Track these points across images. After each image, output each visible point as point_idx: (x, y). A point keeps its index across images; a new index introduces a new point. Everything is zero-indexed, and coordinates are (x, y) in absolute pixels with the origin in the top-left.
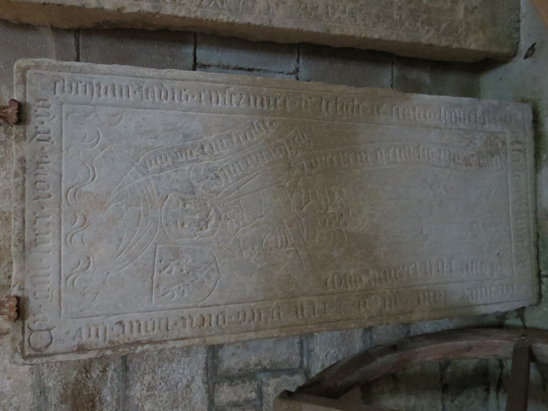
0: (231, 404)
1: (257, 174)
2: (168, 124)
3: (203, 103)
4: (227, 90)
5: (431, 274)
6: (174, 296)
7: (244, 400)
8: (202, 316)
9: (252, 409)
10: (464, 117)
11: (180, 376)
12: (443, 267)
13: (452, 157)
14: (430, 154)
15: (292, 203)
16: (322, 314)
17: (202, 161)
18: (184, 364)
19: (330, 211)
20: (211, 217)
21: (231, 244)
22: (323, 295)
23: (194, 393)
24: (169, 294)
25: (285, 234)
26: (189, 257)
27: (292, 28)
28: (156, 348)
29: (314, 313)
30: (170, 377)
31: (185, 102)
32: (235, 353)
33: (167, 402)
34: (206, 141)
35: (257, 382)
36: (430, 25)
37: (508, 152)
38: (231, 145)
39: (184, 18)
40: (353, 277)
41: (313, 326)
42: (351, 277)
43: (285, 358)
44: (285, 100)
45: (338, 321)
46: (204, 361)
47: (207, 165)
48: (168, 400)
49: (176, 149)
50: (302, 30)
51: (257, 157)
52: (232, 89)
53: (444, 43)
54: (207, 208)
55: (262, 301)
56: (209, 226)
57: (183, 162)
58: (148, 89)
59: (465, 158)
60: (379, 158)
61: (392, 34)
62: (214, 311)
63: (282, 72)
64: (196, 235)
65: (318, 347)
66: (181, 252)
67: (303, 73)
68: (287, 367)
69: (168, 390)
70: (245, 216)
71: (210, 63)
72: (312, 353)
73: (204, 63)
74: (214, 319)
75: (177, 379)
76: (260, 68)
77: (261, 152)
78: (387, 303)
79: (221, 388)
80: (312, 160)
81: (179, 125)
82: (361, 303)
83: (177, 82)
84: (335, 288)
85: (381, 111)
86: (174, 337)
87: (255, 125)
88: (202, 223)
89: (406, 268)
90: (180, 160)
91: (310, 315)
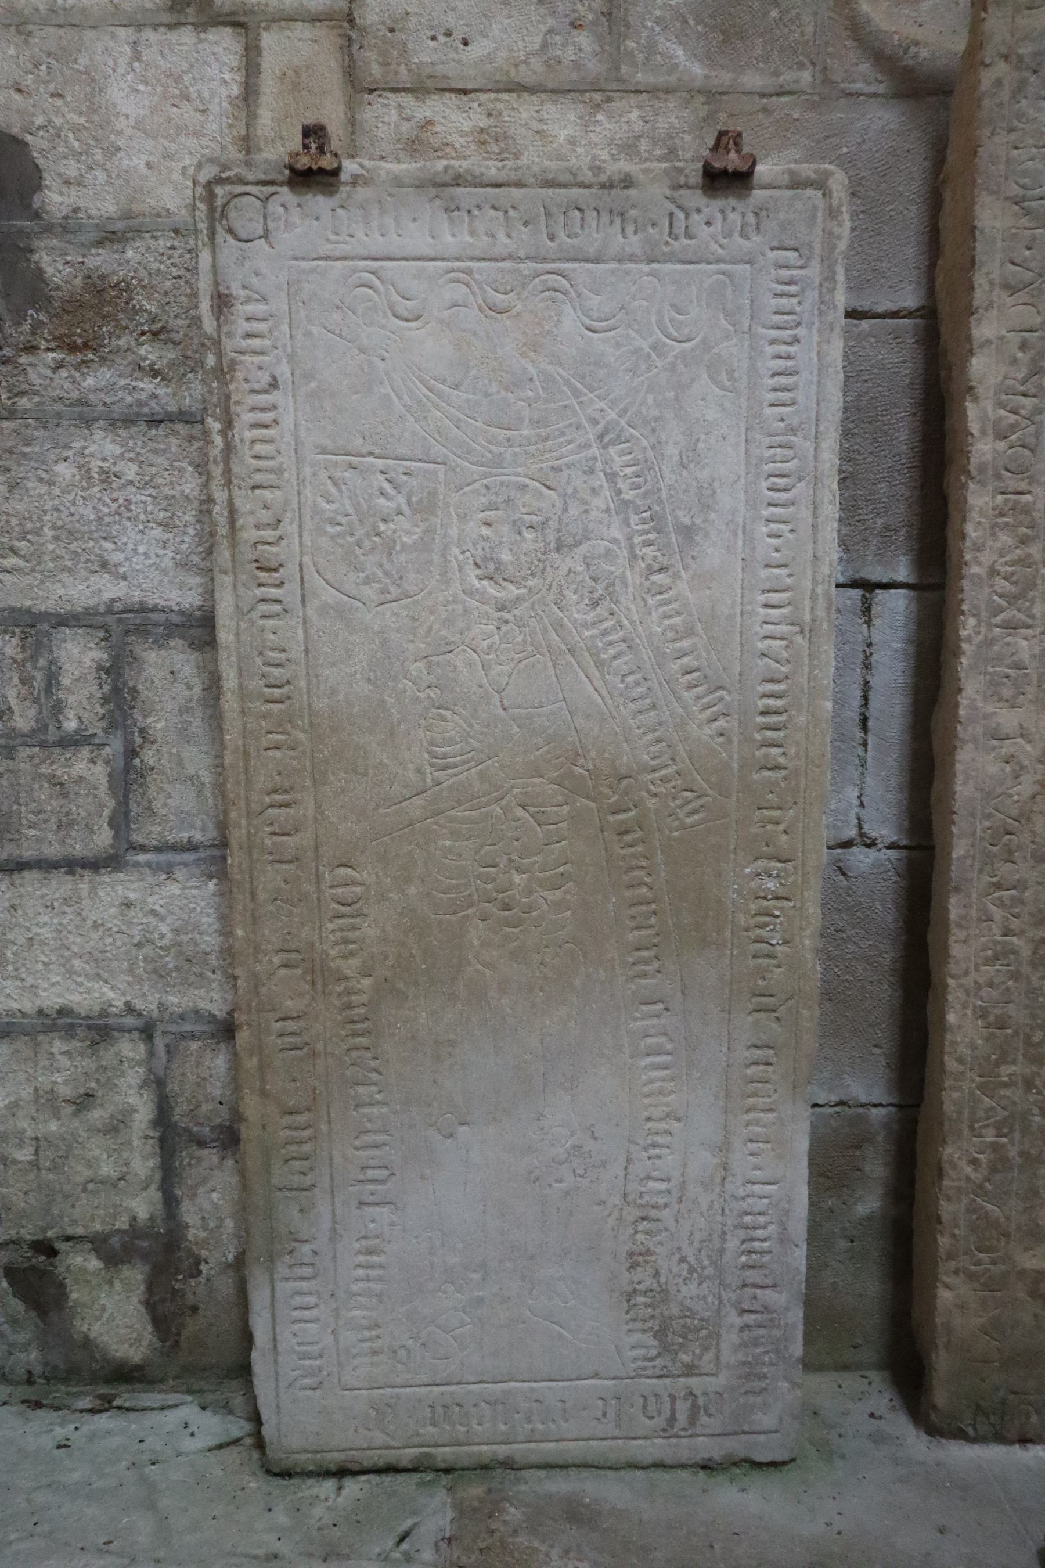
0: (53, 668)
1: (603, 698)
2: (714, 492)
3: (764, 573)
4: (796, 629)
5: (357, 1149)
6: (329, 502)
7: (59, 701)
8: (281, 565)
9: (37, 721)
10: (756, 1253)
11: (130, 546)
12: (372, 1181)
13: (653, 1213)
14: (657, 1151)
15: (536, 780)
16: (271, 853)
17: (632, 567)
18: (157, 556)
19: (517, 879)
20: (504, 588)
21: (443, 633)
22: (317, 857)
23: (87, 579)
24: (333, 490)
25: (464, 763)
26: (415, 537)
27: (957, 797)
28: (215, 461)
29: (274, 834)
30: (128, 524)
31: (764, 529)
32: (175, 680)
33: (72, 515)
34: (676, 576)
35: (102, 734)
36: (993, 1170)
37: (668, 1381)
38: (670, 635)
39: (964, 537)
40: (358, 933)
41: (244, 831)
42: (355, 928)
43: (157, 806)
44: (778, 767)
45: (253, 895)
46: (163, 603)
47: (623, 579)
48: (77, 517)
49: (657, 508)
50: (954, 823)
51: (642, 697)
52: (799, 639)
53: (946, 1209)
54: (525, 578)
55: (310, 705)
56: (484, 582)
57: (629, 526)
58: (790, 448)
59: (649, 1252)
60: (644, 1008)
61: (961, 1060)
62: (290, 593)
63: (862, 805)
64: (463, 552)
65: (177, 892)
66: (427, 520)
67: (861, 859)
68: (134, 809)
69: (100, 519)
70: (506, 668)
71: (876, 622)
72: (164, 876)
73: (875, 609)
74: (274, 592)
75: (125, 539)
76: (869, 747)
77: (654, 707)
78: (291, 1026)
79: (92, 645)
80: (638, 834)
81: (713, 516)
82: (294, 956)
83: (810, 513)
84: (331, 887)
85: (762, 1015)
86: (238, 503)
87: (718, 694)
88: (491, 566)
89: (374, 1076)
90: (634, 518)
91: (272, 824)
